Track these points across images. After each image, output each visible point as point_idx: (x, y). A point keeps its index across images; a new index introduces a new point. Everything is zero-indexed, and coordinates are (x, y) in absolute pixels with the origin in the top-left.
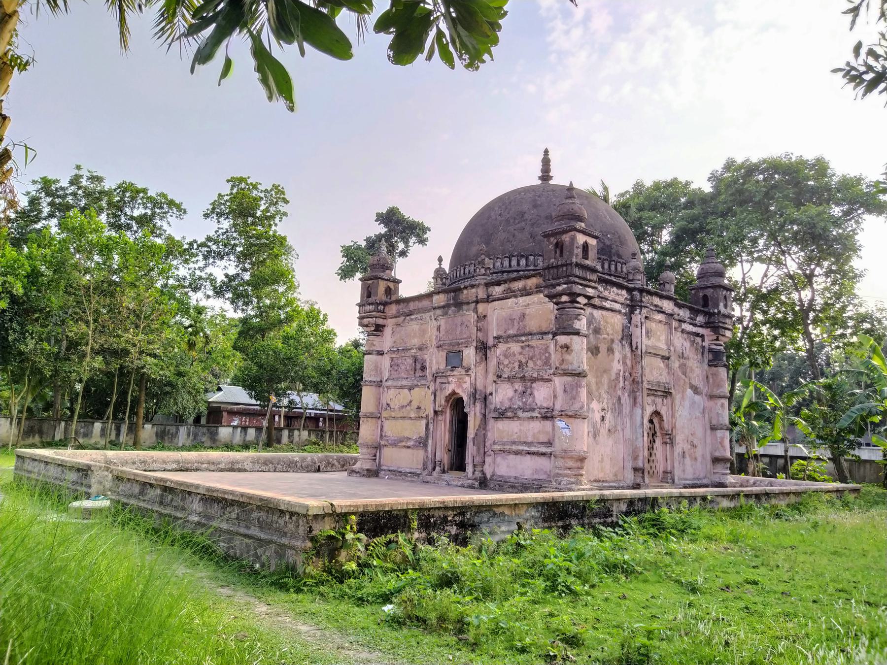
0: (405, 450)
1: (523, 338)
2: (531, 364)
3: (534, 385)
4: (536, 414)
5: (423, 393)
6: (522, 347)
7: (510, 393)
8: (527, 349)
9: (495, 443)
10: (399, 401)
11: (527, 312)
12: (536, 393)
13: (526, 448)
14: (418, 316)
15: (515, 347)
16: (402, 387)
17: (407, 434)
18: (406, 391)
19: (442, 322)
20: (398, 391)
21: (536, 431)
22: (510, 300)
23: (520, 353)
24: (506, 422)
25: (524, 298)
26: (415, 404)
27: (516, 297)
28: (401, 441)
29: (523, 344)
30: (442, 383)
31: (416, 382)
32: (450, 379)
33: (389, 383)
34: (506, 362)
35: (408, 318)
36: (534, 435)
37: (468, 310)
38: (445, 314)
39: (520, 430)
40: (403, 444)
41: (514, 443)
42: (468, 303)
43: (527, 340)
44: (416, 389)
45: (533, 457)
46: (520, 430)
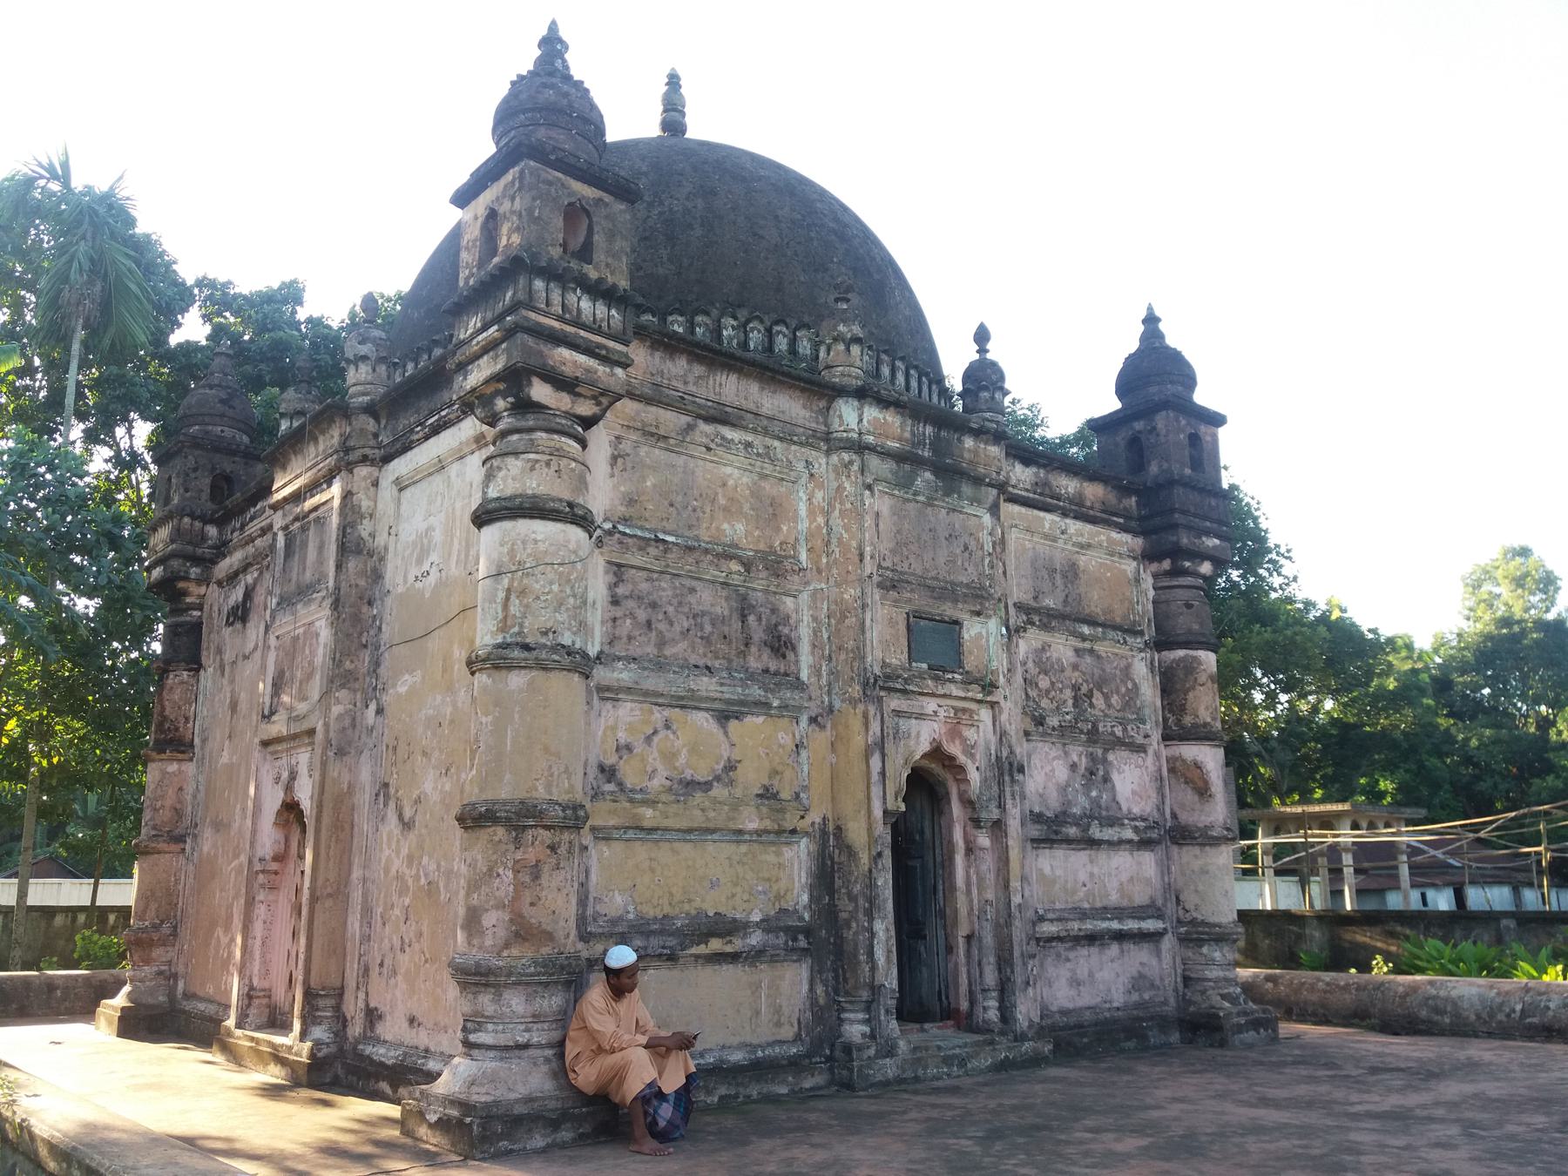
0: (707, 973)
1: (1086, 630)
2: (1098, 700)
3: (1111, 757)
4: (1129, 834)
5: (785, 739)
6: (1077, 651)
7: (1062, 773)
8: (1088, 659)
9: (1041, 919)
10: (669, 757)
11: (1082, 561)
12: (1115, 777)
13: (1115, 925)
14: (758, 441)
15: (1062, 648)
16: (686, 702)
17: (712, 903)
18: (703, 721)
19: (880, 503)
20: (658, 715)
21: (1124, 877)
22: (1049, 516)
23: (1075, 667)
24: (1059, 853)
25: (1079, 525)
26: (751, 777)
27: (1065, 514)
28: (704, 937)
29: (1080, 645)
30: (898, 713)
31: (756, 692)
32: (930, 705)
33: (621, 675)
34: (1044, 683)
35: (708, 428)
36: (1121, 890)
37: (976, 501)
38: (905, 483)
39: (1092, 875)
40: (716, 945)
41: (1083, 915)
42: (978, 481)
43: (1093, 639)
44: (755, 721)
45: (1129, 946)
46: (1092, 875)
